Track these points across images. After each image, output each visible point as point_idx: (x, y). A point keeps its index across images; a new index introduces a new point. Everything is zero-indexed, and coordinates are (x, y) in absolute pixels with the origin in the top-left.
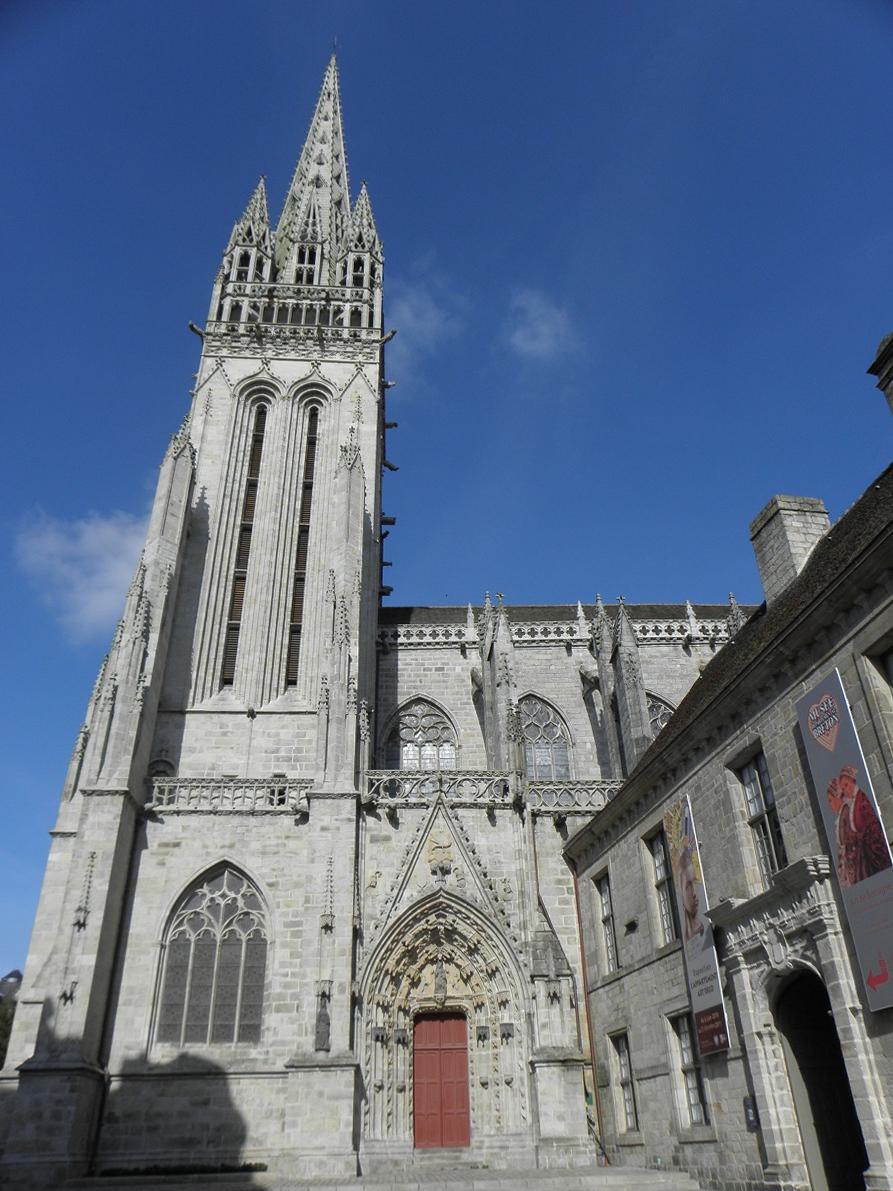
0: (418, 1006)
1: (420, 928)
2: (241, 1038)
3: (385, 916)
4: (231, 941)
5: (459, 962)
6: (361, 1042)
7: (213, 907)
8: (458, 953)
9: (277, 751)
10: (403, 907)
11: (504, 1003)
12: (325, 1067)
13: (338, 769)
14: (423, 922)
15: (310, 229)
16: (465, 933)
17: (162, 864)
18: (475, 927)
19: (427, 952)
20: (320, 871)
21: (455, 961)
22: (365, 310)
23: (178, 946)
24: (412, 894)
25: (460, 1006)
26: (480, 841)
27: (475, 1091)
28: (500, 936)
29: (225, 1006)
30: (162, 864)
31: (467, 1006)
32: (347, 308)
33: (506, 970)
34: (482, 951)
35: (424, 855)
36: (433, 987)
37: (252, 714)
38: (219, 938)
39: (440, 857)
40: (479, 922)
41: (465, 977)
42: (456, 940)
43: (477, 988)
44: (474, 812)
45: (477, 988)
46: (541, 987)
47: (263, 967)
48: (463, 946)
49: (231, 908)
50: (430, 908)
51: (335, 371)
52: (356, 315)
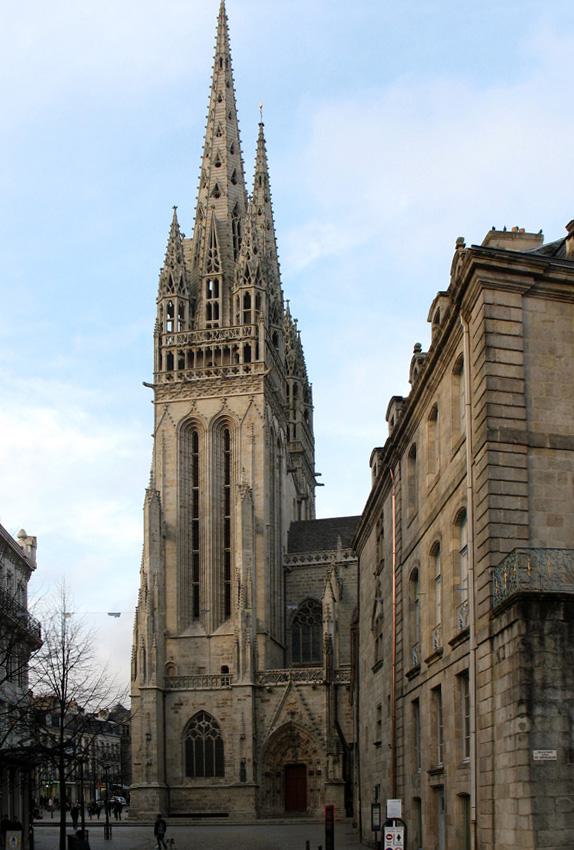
2: (217, 776)
4: (209, 740)
6: (259, 779)
7: (200, 728)
9: (222, 655)
10: (275, 729)
11: (318, 763)
12: (245, 787)
13: (244, 673)
15: (213, 259)
17: (177, 712)
20: (238, 717)
22: (252, 344)
23: (188, 743)
24: (279, 723)
26: (310, 701)
27: (308, 792)
29: (209, 764)
30: (177, 712)
32: (241, 345)
35: (285, 707)
37: (209, 637)
38: (204, 739)
39: (291, 708)
44: (307, 688)
46: (331, 758)
47: (223, 751)
49: (207, 728)
51: (237, 405)
52: (247, 349)
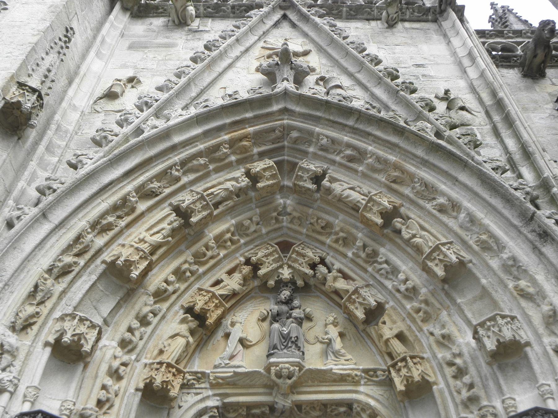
0: (213, 403)
1: (228, 185)
3: (127, 129)
5: (341, 284)
8: (337, 265)
14: (239, 173)
16: (355, 196)
18: (382, 178)
19: (248, 262)
21: (330, 282)
25: (349, 405)
28: (463, 177)
31: (372, 403)
33: (494, 263)
34: (406, 235)
36: (260, 351)
40: (392, 158)
41: (360, 314)
42: (327, 227)
43: (398, 347)
45: (398, 347)
48: (347, 241)
50: (257, 138)
